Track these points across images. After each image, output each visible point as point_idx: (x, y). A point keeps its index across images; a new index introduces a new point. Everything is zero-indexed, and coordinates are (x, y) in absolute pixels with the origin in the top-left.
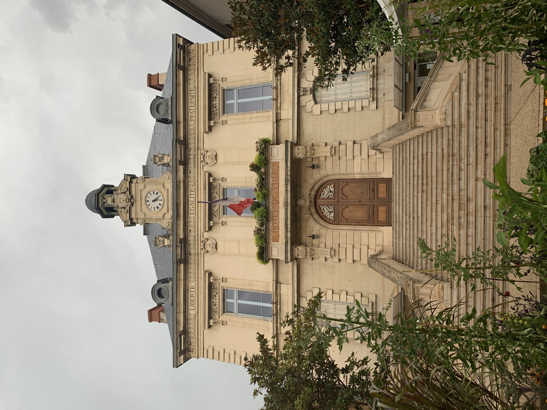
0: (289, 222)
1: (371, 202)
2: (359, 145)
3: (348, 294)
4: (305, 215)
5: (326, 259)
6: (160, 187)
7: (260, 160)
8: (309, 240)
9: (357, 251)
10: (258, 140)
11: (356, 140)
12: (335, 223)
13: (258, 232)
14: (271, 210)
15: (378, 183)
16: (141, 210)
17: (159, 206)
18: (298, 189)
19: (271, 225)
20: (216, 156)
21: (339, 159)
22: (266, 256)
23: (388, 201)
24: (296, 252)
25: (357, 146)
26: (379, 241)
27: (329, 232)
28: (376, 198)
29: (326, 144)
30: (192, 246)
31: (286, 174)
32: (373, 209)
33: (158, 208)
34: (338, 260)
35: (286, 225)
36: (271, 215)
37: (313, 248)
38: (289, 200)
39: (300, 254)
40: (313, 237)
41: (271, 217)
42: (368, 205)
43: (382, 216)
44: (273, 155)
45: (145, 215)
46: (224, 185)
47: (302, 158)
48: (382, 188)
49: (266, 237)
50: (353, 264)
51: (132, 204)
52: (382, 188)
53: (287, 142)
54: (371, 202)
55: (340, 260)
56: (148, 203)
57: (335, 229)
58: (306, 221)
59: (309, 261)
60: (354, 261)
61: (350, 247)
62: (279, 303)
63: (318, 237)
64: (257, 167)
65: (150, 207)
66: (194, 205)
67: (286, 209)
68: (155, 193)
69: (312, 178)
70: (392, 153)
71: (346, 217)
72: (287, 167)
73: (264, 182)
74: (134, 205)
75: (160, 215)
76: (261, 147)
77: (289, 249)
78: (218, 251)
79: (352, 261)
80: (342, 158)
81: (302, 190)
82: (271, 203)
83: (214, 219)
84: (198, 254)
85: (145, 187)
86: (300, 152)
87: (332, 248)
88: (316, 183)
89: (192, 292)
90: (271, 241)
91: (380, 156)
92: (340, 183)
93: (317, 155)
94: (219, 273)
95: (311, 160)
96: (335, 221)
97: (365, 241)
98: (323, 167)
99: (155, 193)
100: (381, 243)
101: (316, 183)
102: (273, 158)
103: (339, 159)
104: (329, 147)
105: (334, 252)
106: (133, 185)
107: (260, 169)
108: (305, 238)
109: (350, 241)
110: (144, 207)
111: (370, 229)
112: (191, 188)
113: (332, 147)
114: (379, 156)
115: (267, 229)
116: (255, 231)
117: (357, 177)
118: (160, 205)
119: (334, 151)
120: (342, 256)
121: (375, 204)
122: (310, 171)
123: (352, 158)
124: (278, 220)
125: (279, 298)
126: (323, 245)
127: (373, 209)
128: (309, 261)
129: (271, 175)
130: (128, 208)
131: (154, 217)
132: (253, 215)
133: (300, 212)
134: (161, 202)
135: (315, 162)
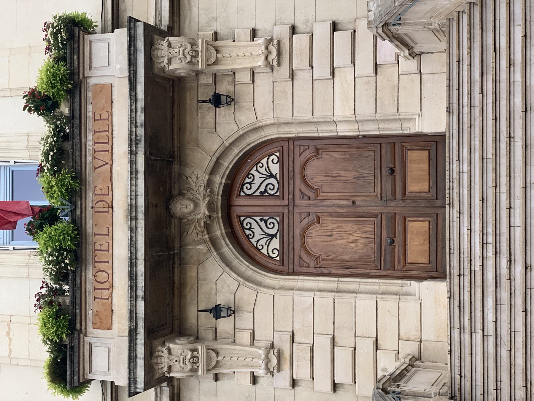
0: (141, 268)
2: (349, 33)
5: (255, 380)
7: (53, 78)
8: (206, 319)
9: (343, 356)
10: (52, 20)
11: (342, 18)
12: (285, 268)
13: (49, 300)
14: (89, 230)
15: (404, 150)
19: (90, 276)
21: (292, 76)
22: (72, 374)
23: (434, 204)
24: (164, 361)
25: (342, 38)
26: (410, 327)
28: (399, 195)
29: (254, 34)
31: (133, 121)
32: (392, 228)
34: (287, 383)
35: (132, 276)
36: (90, 247)
37: (217, 346)
38: (141, 201)
39: (176, 367)
40: (217, 312)
41: (90, 253)
42: (375, 215)
43: (417, 249)
44: (94, 65)
47: (182, 73)
48: (417, 163)
49: (74, 315)
50: (332, 395)
52: (417, 163)
53: (133, 21)
55: (294, 383)
57: (281, 288)
59: (206, 383)
60: (335, 387)
61: (323, 345)
63: (231, 311)
64: (45, 99)
67: (133, 230)
69: (216, 135)
70: (445, 56)
71: (315, 251)
72: (133, 98)
73: (67, 146)
76: (56, 39)
77: (140, 350)
79: (328, 387)
80: (299, 75)
82: (90, 211)
86: (174, 56)
87: (272, 346)
88: (227, 150)
90: (90, 325)
92: (297, 152)
93: (227, 66)
96: (282, 261)
97: (367, 326)
98: (245, 102)
100: (414, 334)
101: (227, 150)
102: (94, 73)
103: (292, 76)
105: (277, 358)
107: (56, 105)
109: (324, 325)
111: (383, 288)
115: (78, 292)
116: (40, 297)
120: (302, 371)
121: (398, 211)
123: (328, 75)
124: (110, 262)
126: (246, 337)
127: (392, 228)
129: (90, 125)
132: (35, 245)
133: (181, 235)
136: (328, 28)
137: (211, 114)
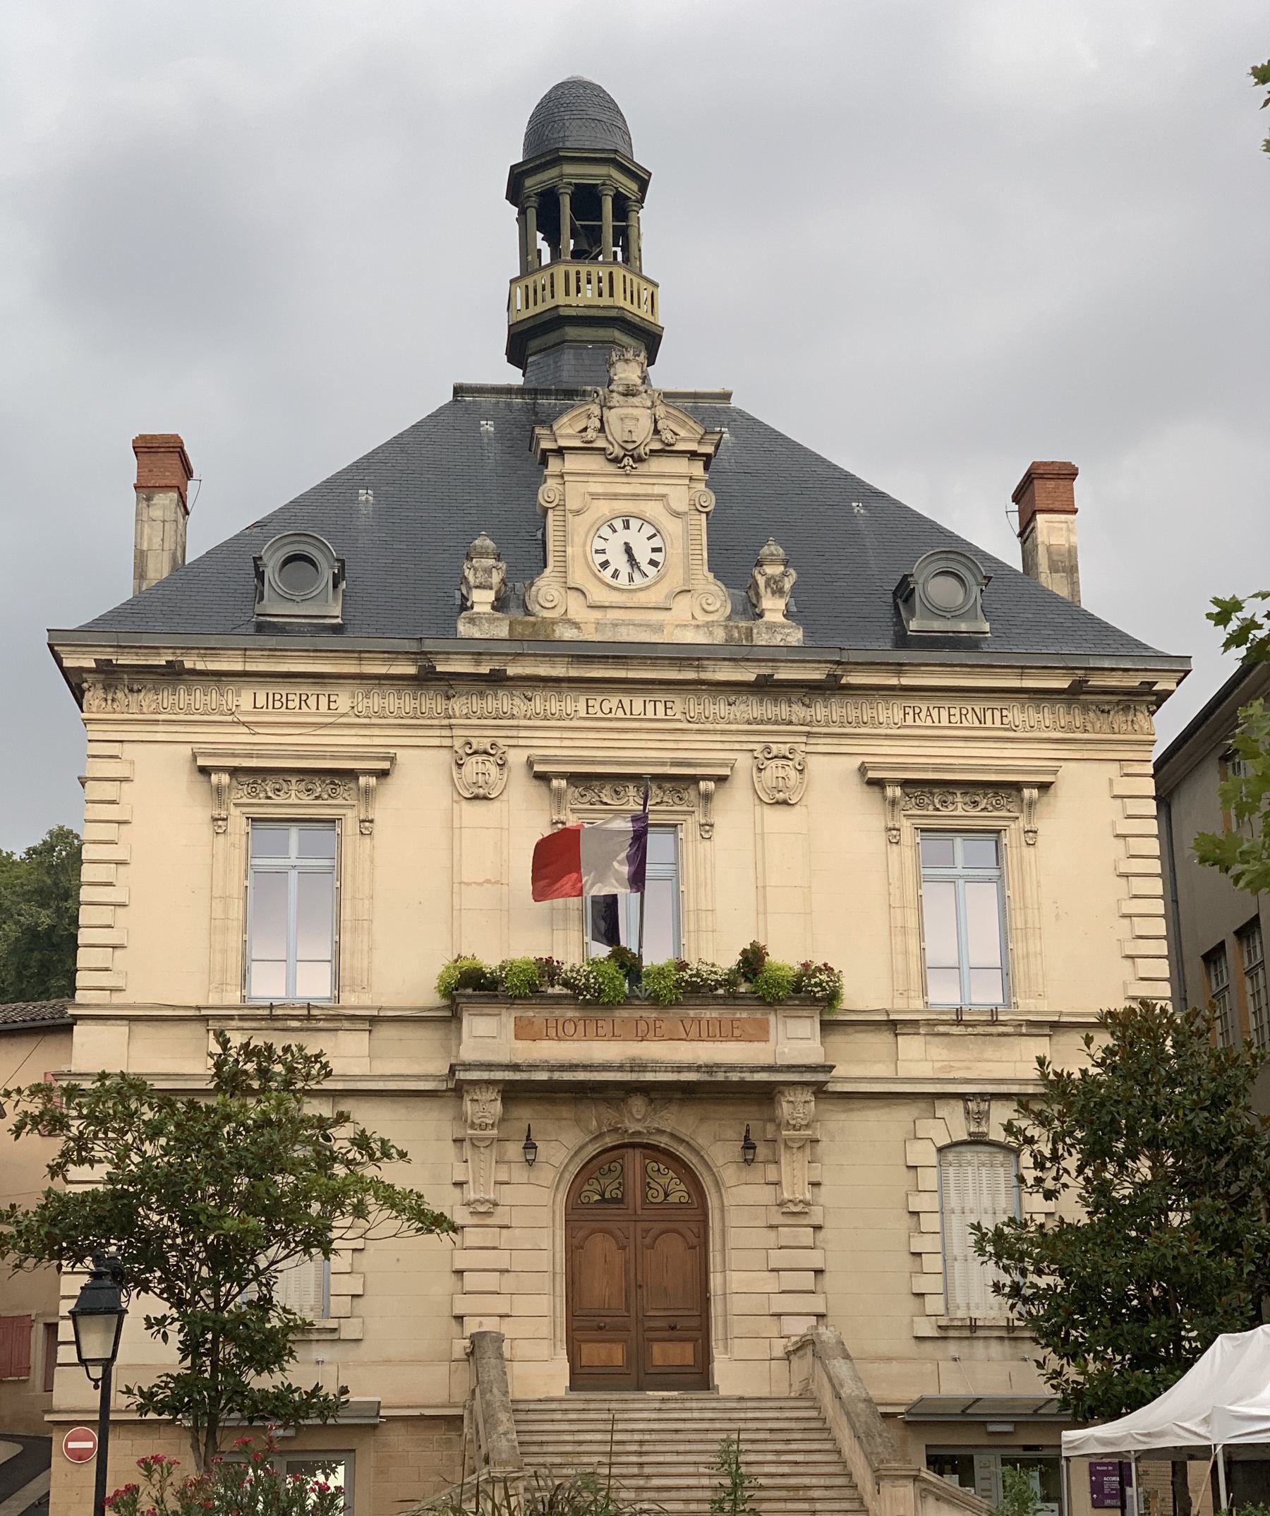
1: (643, 1321)
3: (357, 1254)
4: (595, 1117)
6: (675, 579)
9: (491, 1281)
16: (595, 496)
17: (610, 571)
18: (679, 1096)
20: (785, 803)
21: (771, 1227)
27: (545, 1196)
29: (816, 1184)
30: (476, 704)
33: (605, 565)
45: (578, 513)
46: (689, 828)
48: (681, 1354)
51: (616, 460)
52: (681, 1354)
54: (643, 1321)
56: (618, 524)
58: (577, 1121)
60: (459, 1273)
62: (305, 1024)
65: (605, 531)
66: (620, 714)
68: (657, 557)
74: (611, 468)
75: (578, 576)
78: (464, 803)
79: (458, 1266)
80: (772, 1234)
81: (674, 1108)
83: (573, 793)
84: (450, 727)
85: (677, 515)
87: (496, 1205)
88: (698, 1154)
89: (316, 703)
91: (779, 1352)
94: (390, 805)
95: (769, 1136)
97: (522, 1305)
99: (657, 557)
101: (698, 1154)
103: (771, 1227)
104: (808, 1196)
106: (681, 466)
108: (525, 1115)
109: (521, 1261)
110: (604, 508)
112: (679, 705)
113: (808, 1204)
114: (779, 1348)
117: (715, 1281)
118: (615, 575)
119: (795, 1212)
122: (734, 1134)
125: (321, 1024)
128: (449, 1130)
130: (600, 443)
131: (569, 550)
134: (623, 580)
135: (762, 1151)
136: (818, 1266)
137: (735, 1136)
